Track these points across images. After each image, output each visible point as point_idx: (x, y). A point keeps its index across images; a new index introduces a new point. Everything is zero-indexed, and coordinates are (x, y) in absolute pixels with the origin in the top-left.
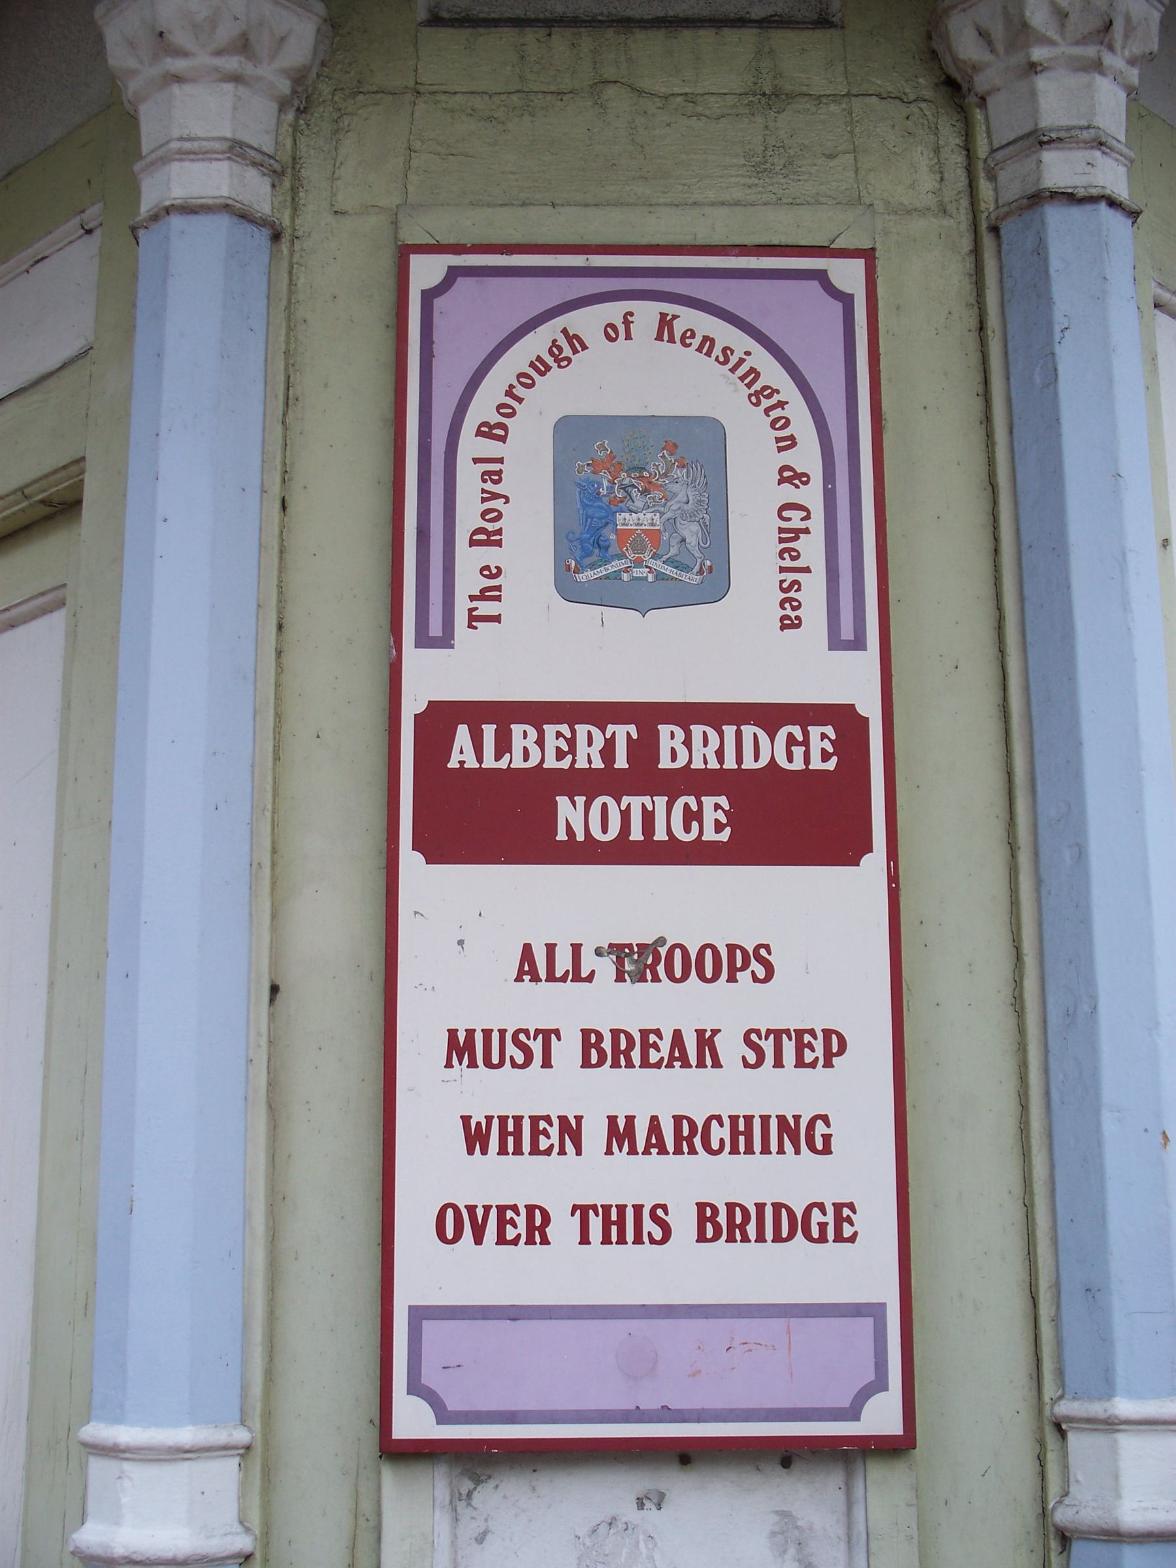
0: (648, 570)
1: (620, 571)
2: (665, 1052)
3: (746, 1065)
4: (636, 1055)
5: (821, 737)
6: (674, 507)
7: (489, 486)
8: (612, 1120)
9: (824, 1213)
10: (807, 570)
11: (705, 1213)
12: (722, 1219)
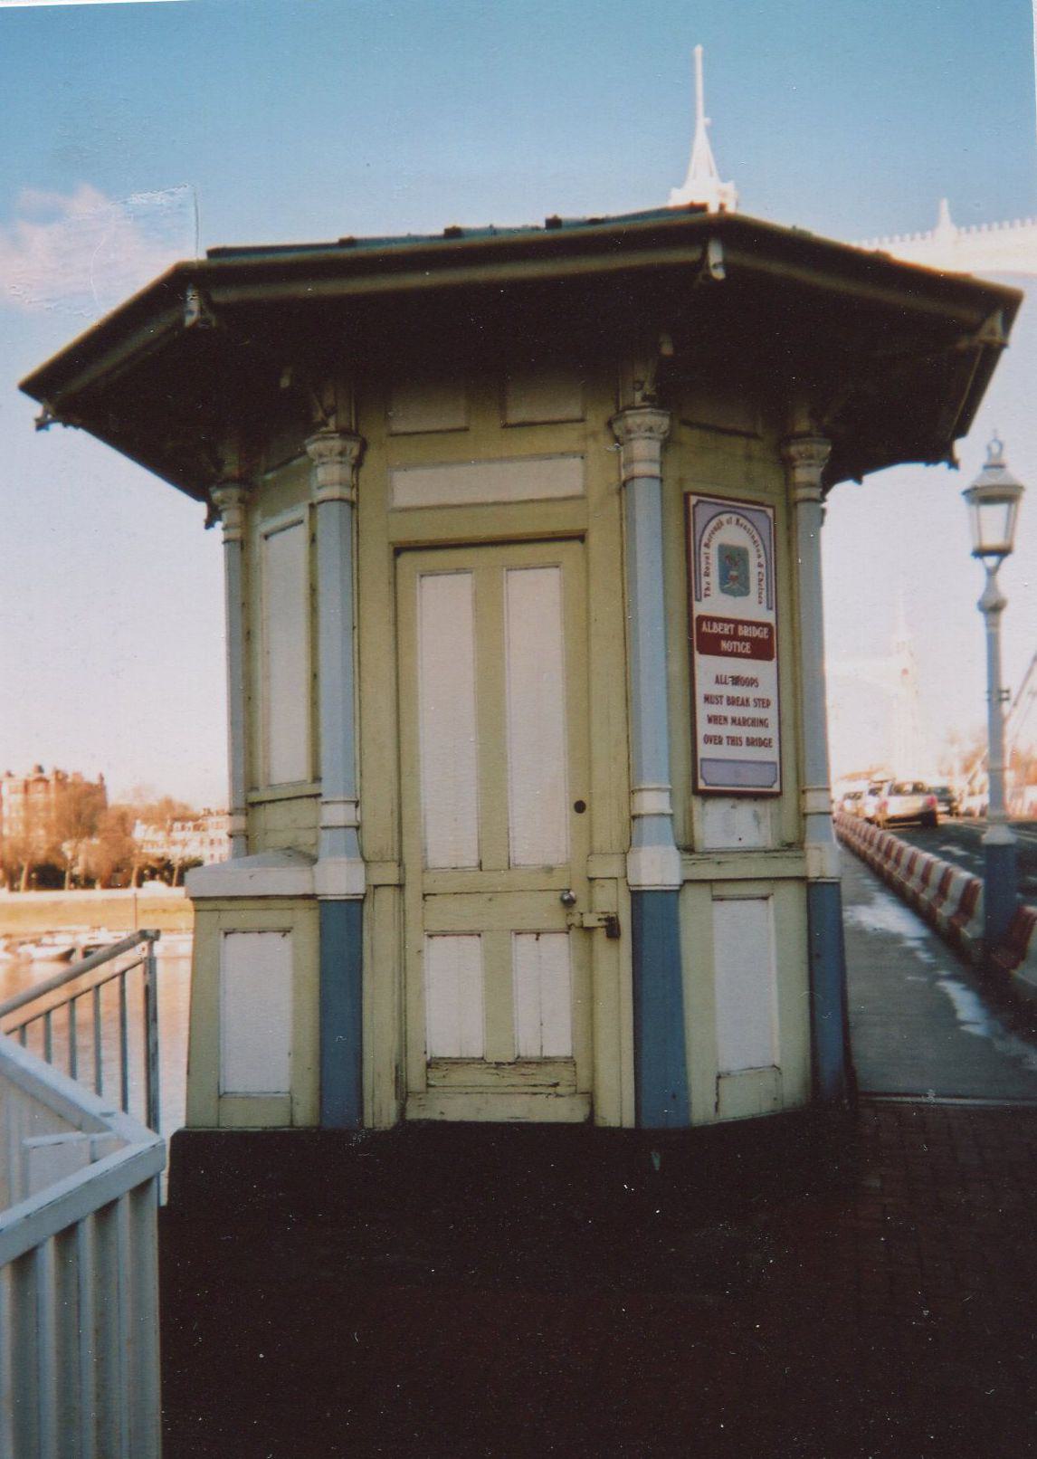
5: (766, 630)
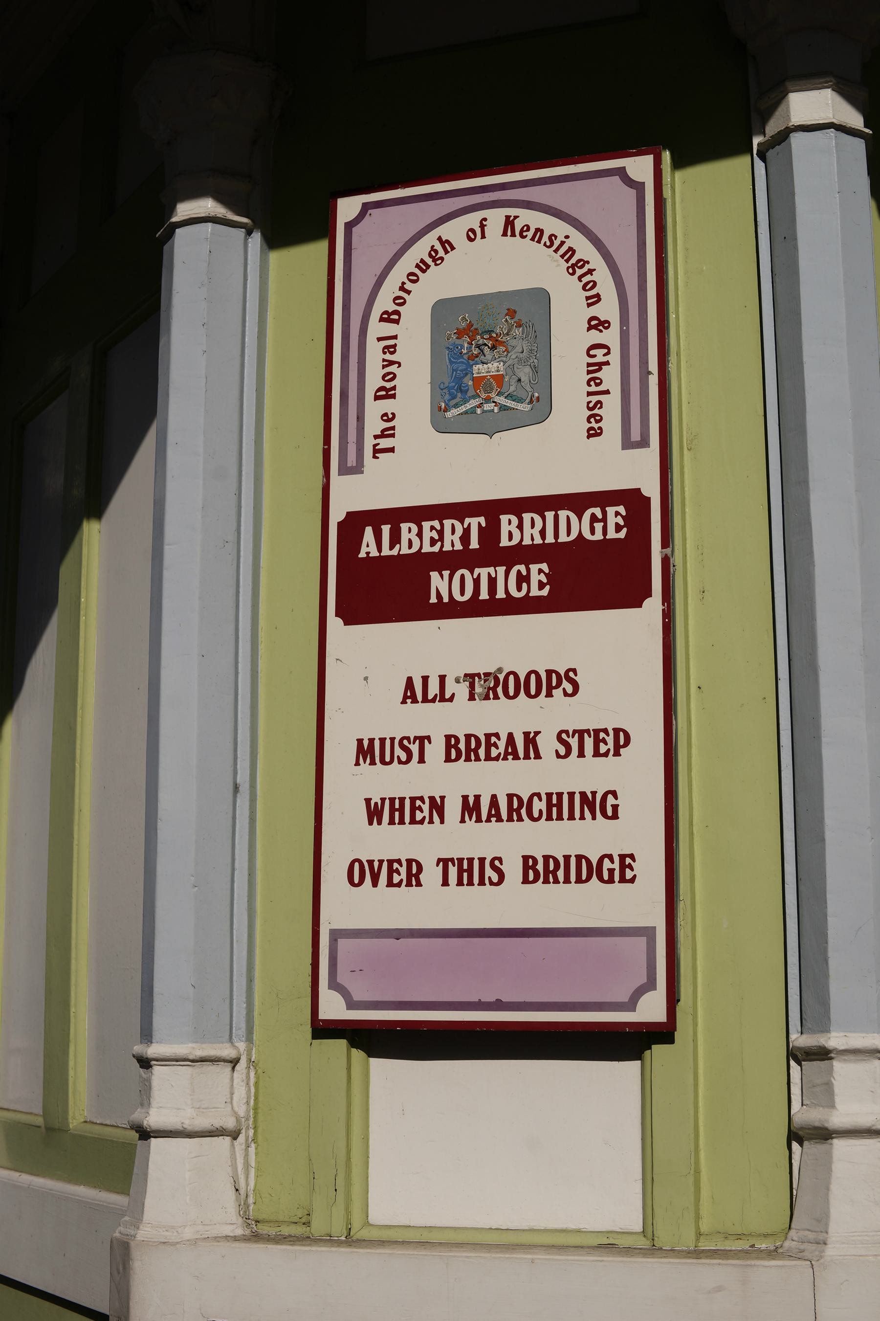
0: (494, 404)
1: (475, 407)
2: (502, 749)
3: (558, 756)
4: (482, 752)
5: (615, 514)
6: (513, 357)
7: (388, 357)
8: (465, 798)
9: (612, 862)
10: (607, 392)
11: (528, 862)
12: (540, 867)
